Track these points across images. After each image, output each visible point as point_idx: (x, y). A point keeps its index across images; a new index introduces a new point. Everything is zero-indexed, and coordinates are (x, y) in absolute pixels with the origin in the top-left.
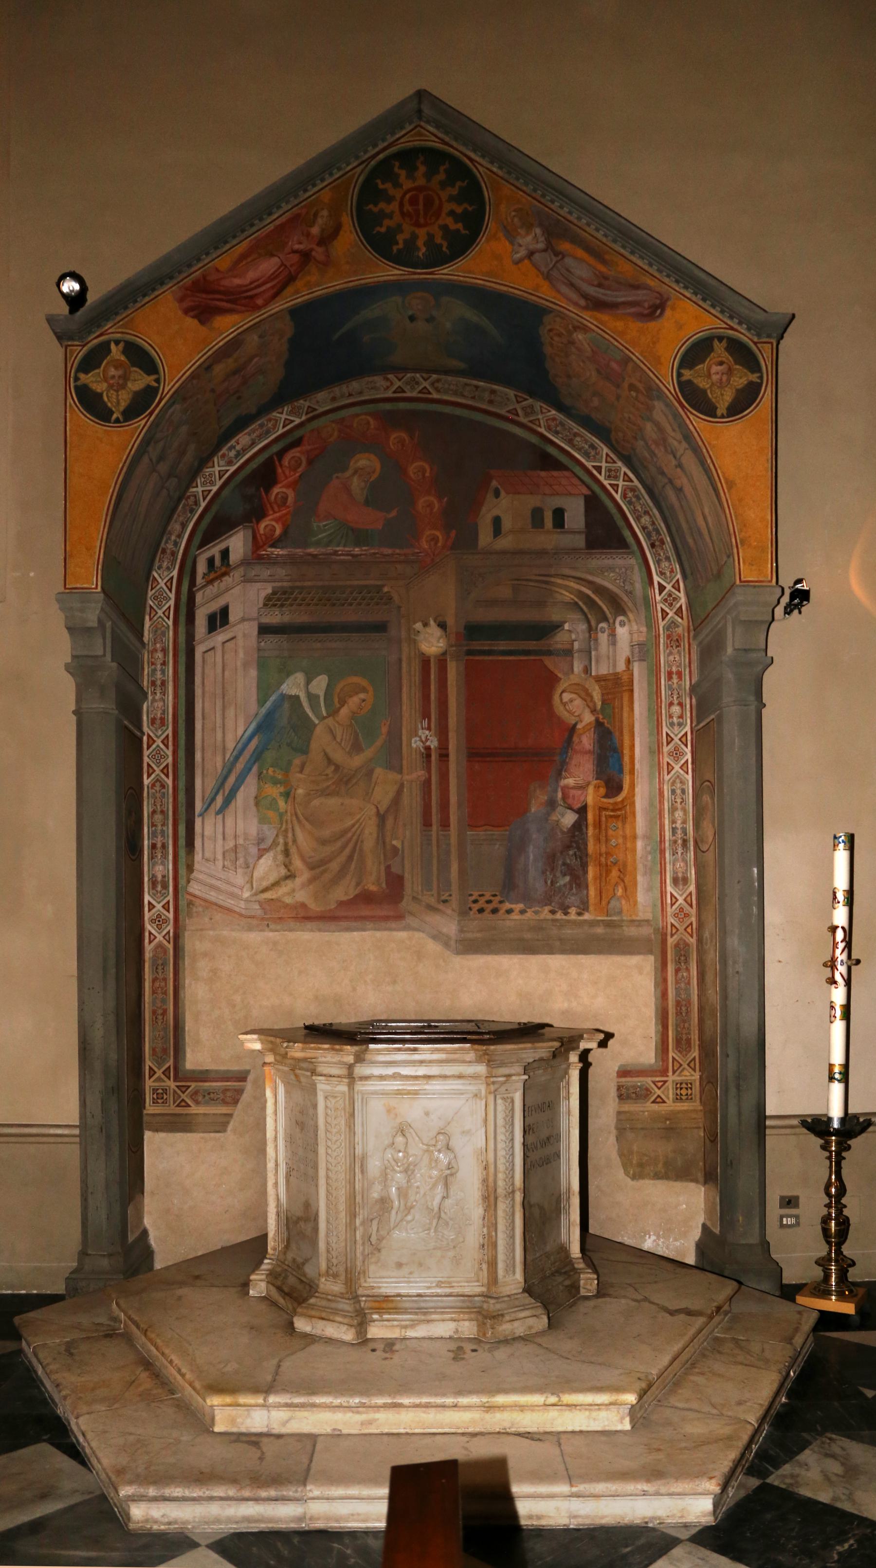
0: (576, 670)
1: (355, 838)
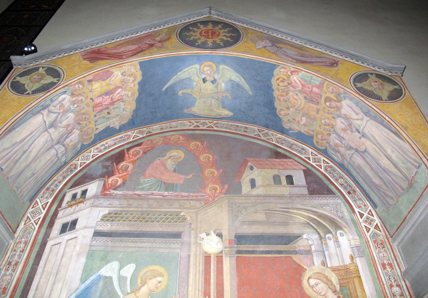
0: (316, 263)
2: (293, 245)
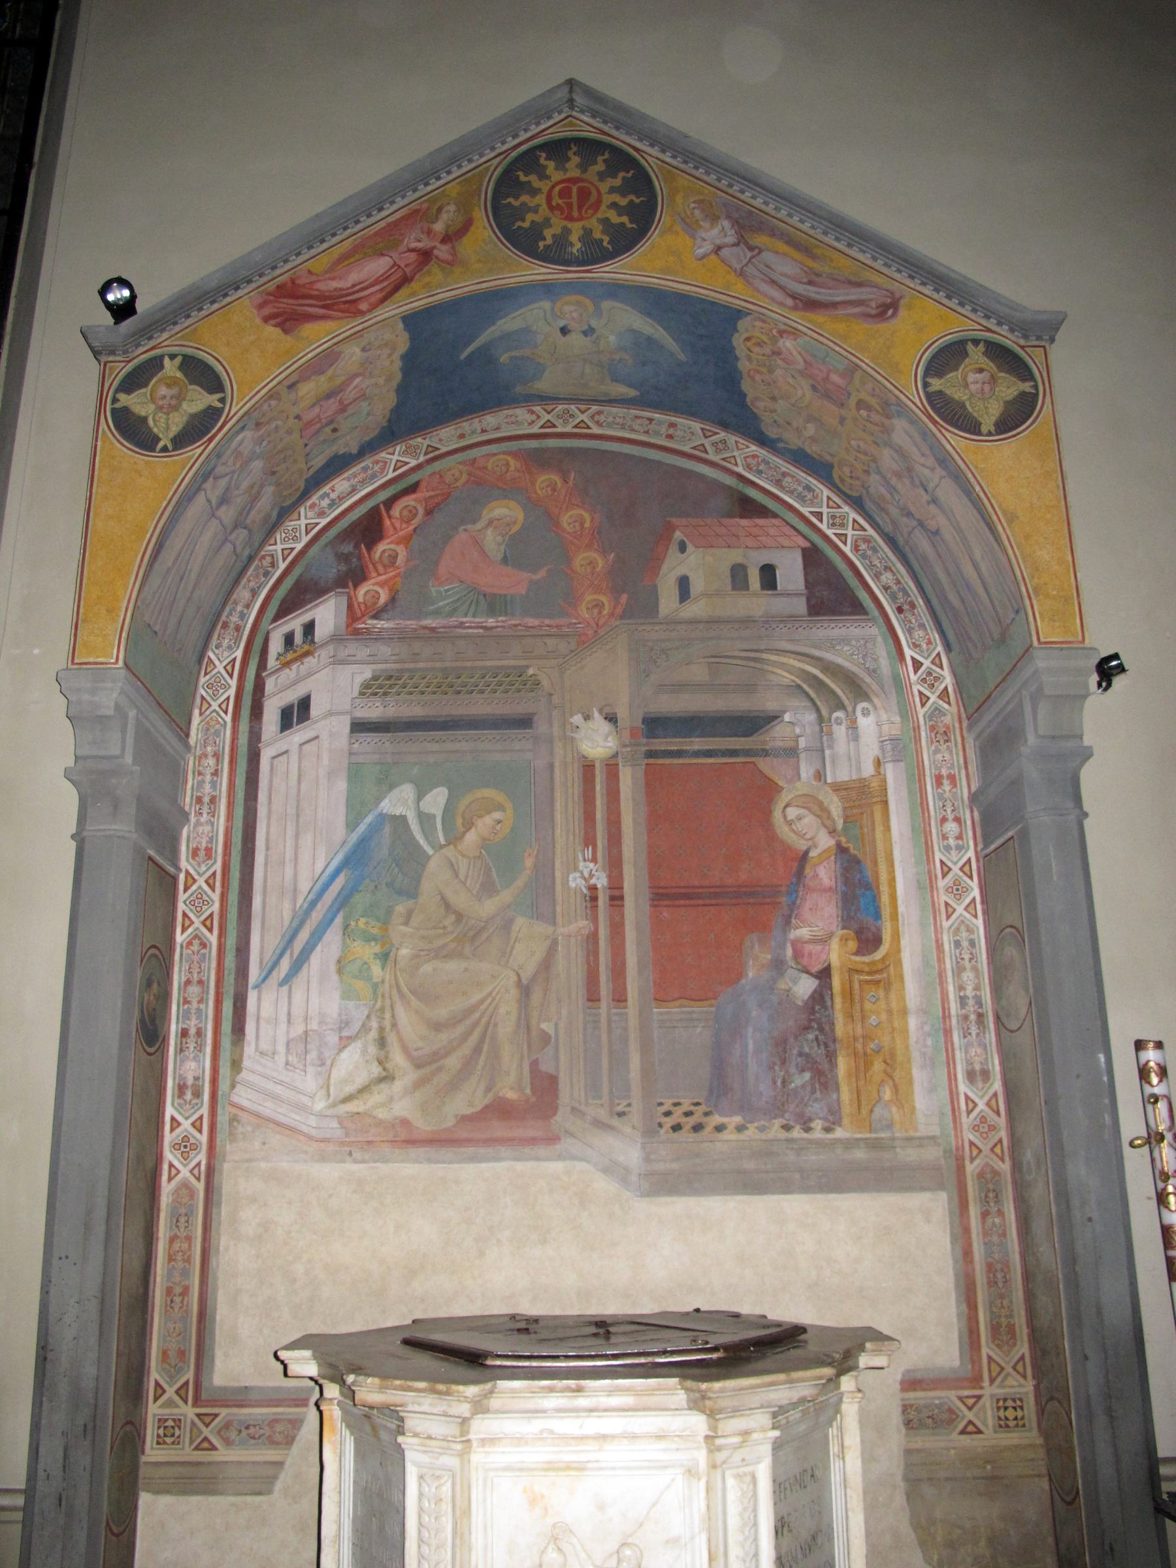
0: (803, 775)
1: (484, 1021)
2: (761, 738)
